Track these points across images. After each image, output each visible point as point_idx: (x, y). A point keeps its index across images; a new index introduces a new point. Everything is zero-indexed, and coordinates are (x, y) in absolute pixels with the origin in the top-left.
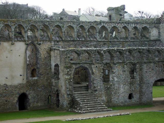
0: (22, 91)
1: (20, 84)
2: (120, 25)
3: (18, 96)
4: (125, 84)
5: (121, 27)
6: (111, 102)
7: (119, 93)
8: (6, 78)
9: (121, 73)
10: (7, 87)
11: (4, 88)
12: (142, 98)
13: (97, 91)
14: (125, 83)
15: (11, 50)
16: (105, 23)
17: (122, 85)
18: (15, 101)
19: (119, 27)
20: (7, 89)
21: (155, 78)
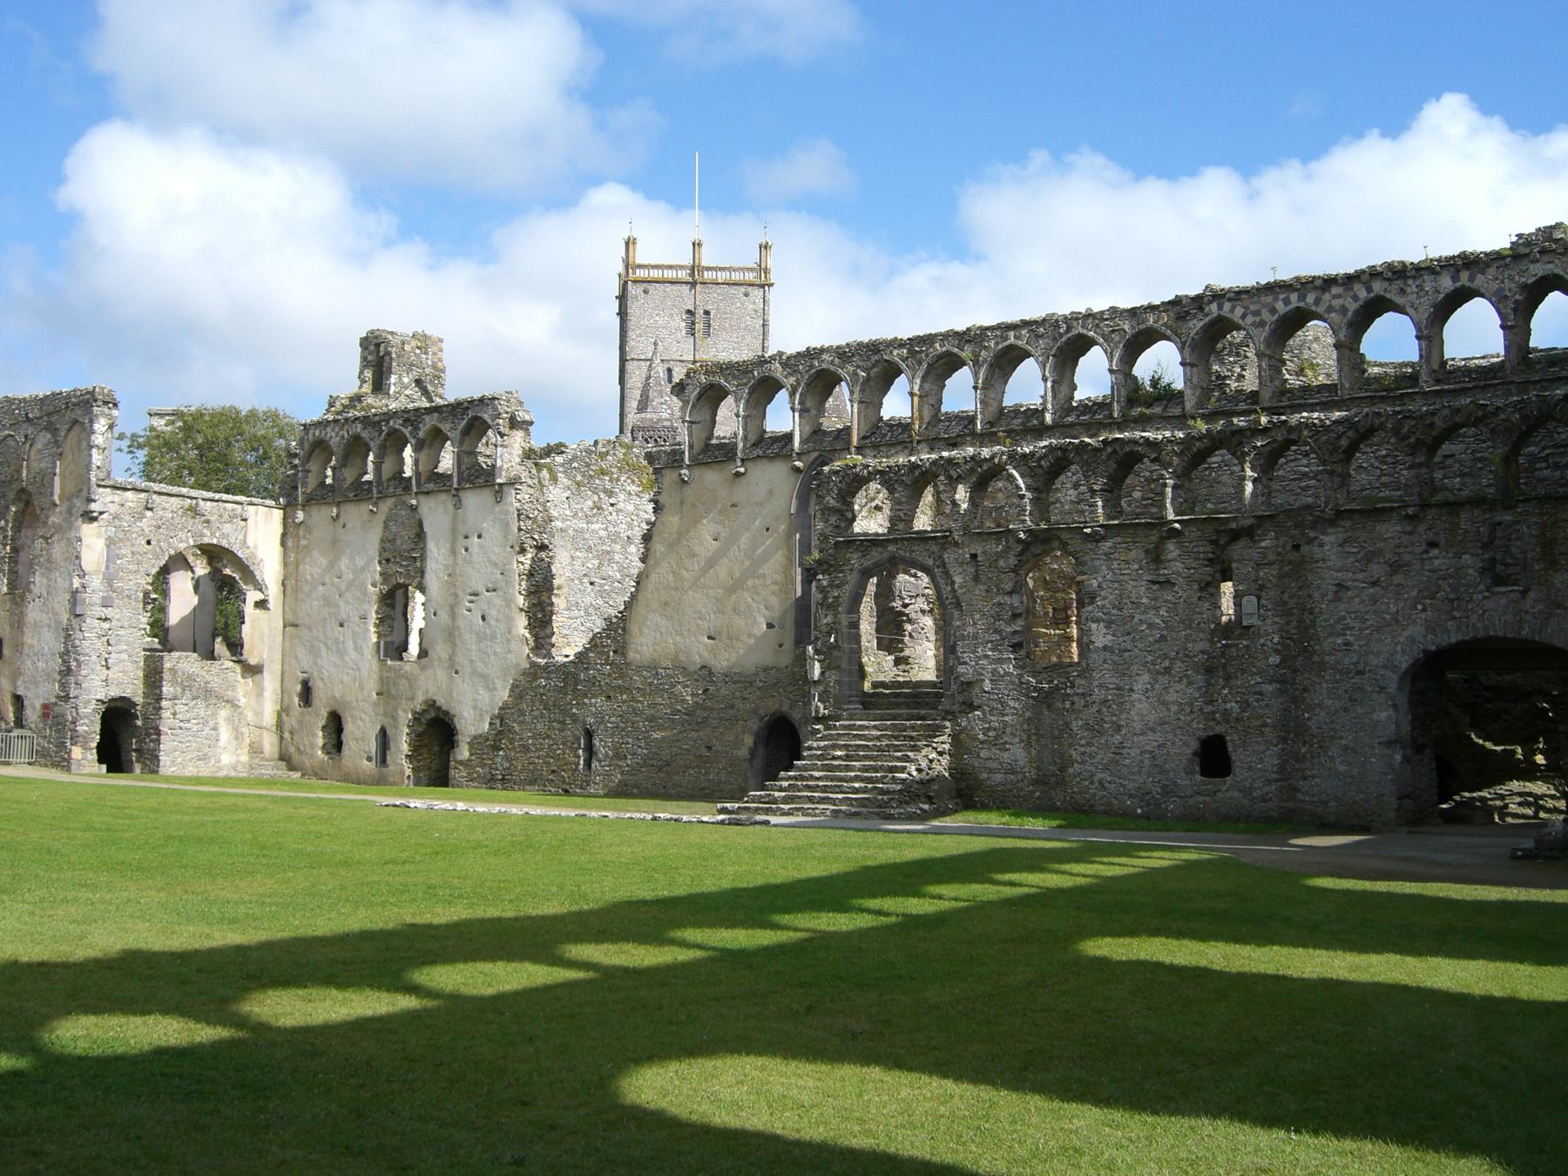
0: (772, 705)
1: (766, 669)
2: (1335, 297)
3: (754, 725)
4: (1167, 670)
5: (1344, 310)
6: (1061, 782)
7: (1118, 728)
8: (709, 638)
9: (1139, 590)
12: (1305, 778)
13: (978, 707)
14: (1167, 663)
15: (733, 506)
16: (1230, 300)
17: (1146, 677)
18: (743, 752)
19: (1330, 309)
21: (1416, 630)
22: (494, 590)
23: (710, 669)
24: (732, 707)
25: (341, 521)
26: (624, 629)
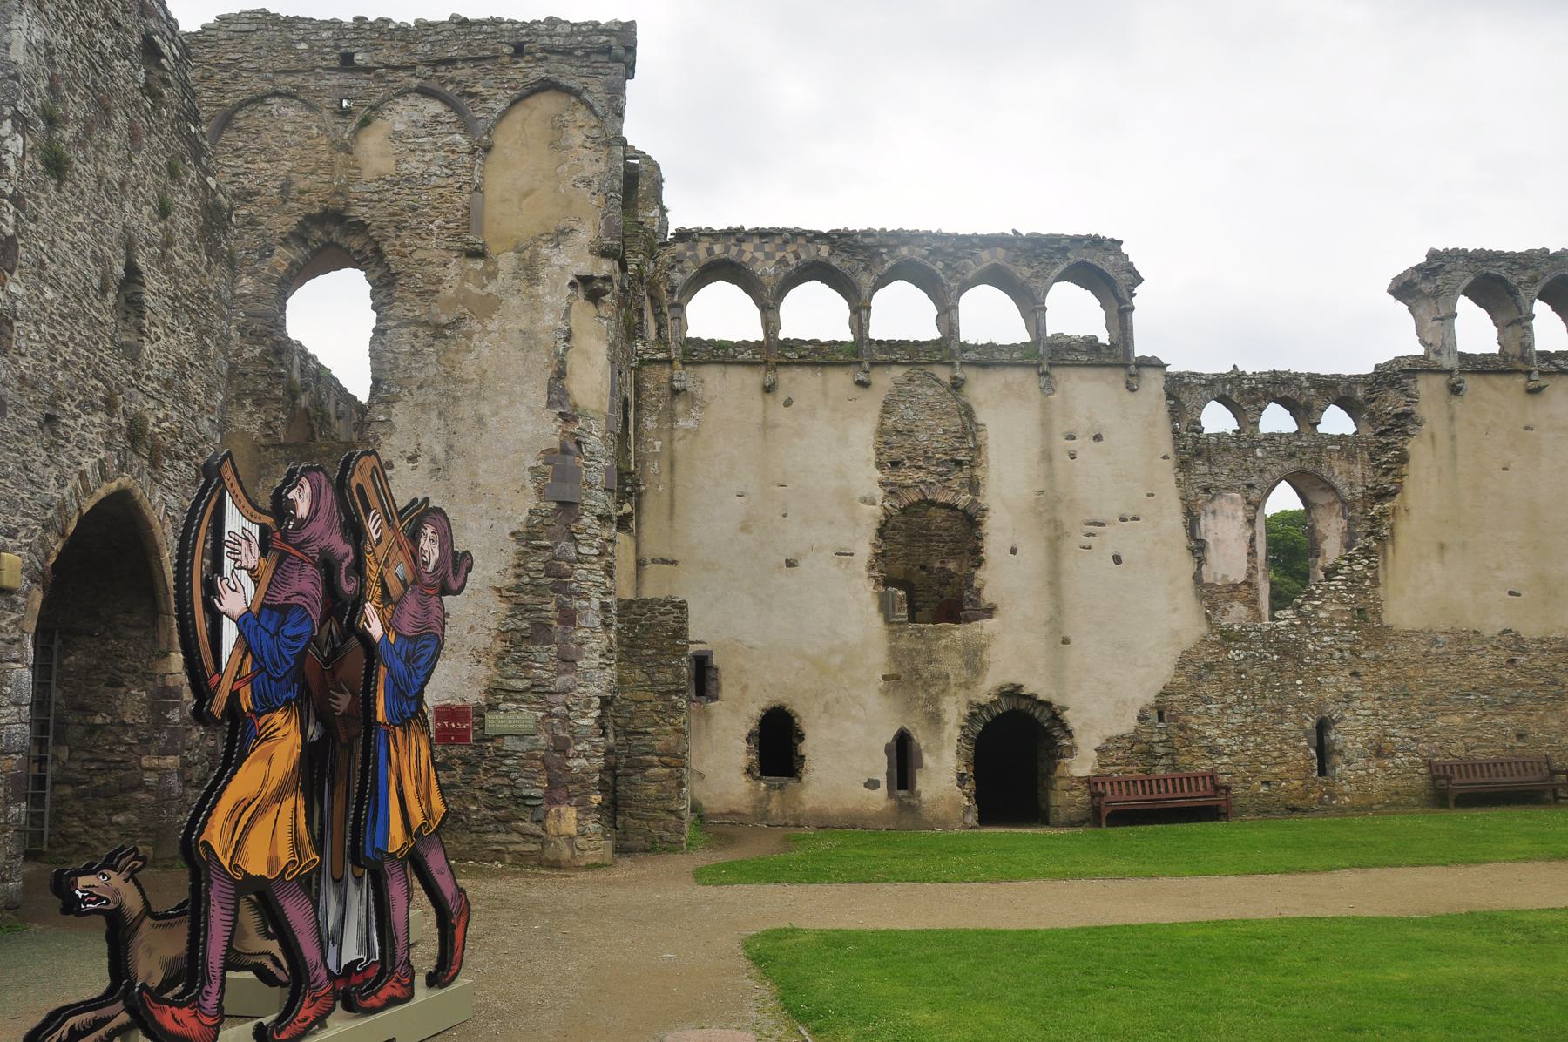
8: (1512, 593)
10: (1523, 651)
11: (1503, 655)
15: (1527, 428)
20: (1522, 659)
22: (1136, 519)
23: (1517, 634)
24: (1554, 682)
25: (782, 395)
26: (1375, 580)
